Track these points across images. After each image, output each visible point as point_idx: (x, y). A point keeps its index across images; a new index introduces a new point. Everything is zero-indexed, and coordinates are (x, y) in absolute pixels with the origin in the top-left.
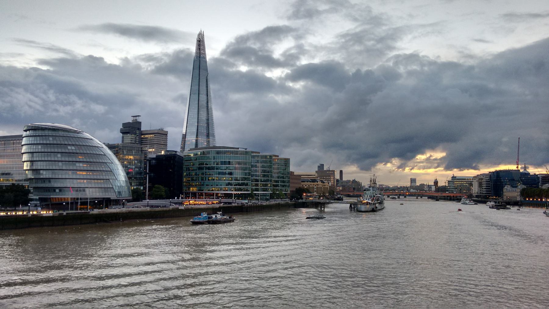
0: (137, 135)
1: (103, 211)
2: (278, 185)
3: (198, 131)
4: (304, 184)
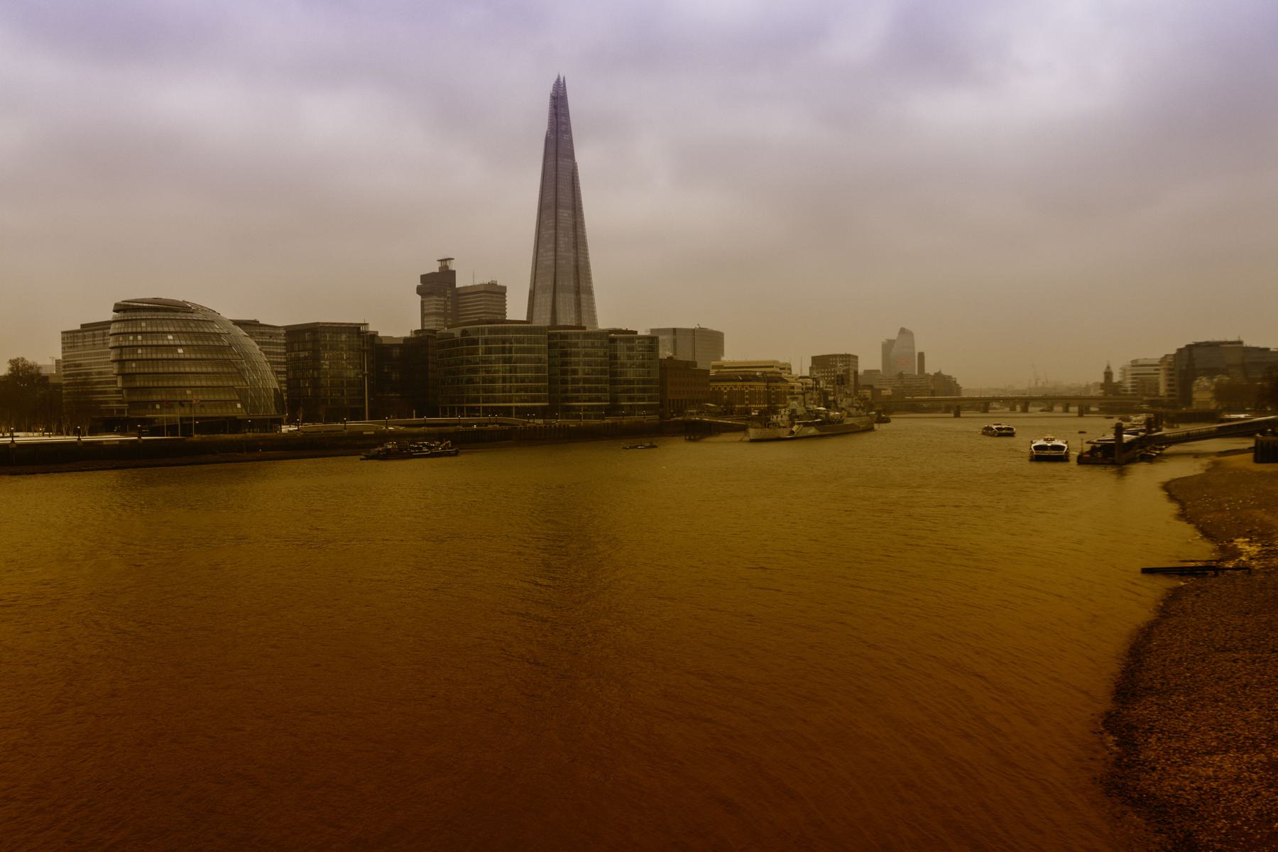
0: (449, 298)
2: (633, 389)
3: (557, 282)
4: (722, 386)
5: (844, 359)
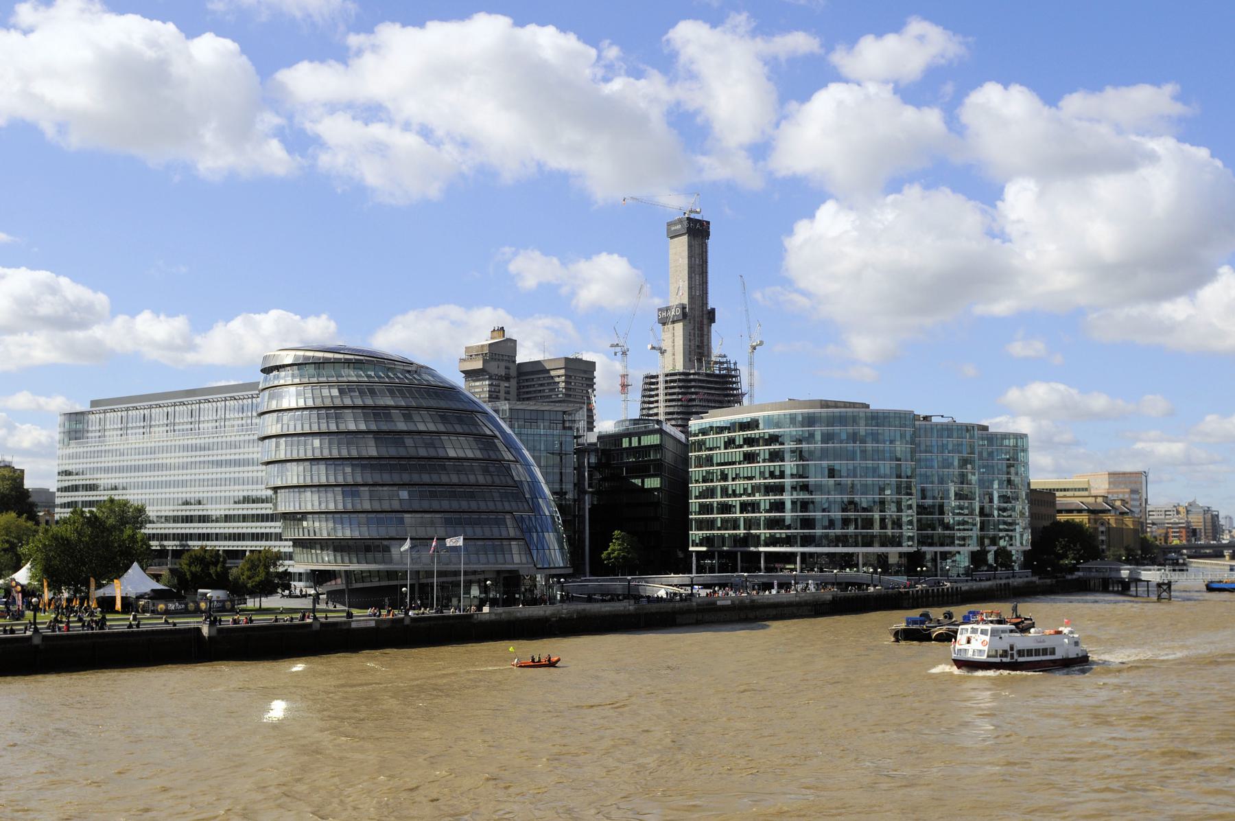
1: (509, 613)
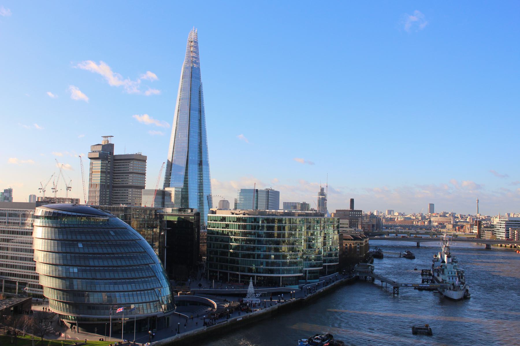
0: (109, 162)
3: (189, 158)
5: (359, 213)
